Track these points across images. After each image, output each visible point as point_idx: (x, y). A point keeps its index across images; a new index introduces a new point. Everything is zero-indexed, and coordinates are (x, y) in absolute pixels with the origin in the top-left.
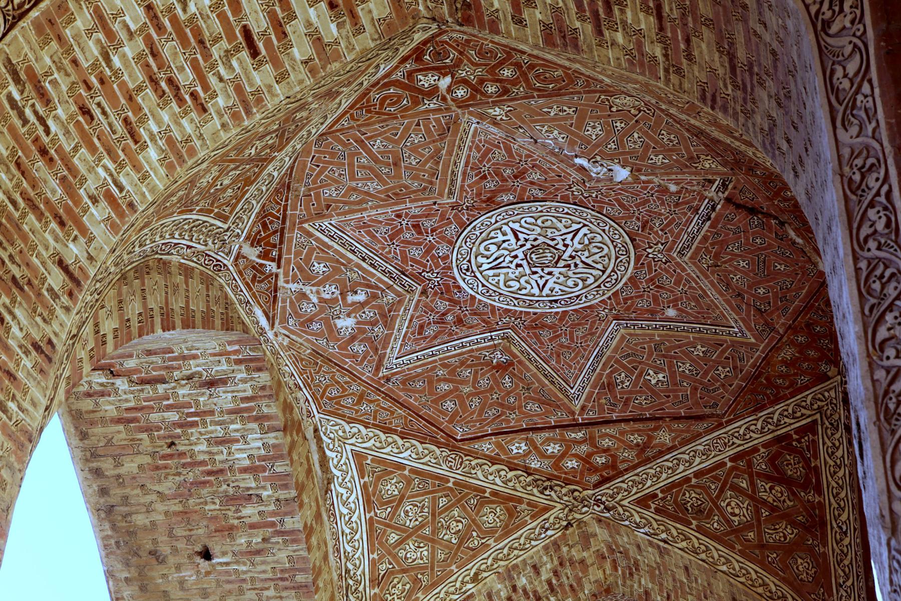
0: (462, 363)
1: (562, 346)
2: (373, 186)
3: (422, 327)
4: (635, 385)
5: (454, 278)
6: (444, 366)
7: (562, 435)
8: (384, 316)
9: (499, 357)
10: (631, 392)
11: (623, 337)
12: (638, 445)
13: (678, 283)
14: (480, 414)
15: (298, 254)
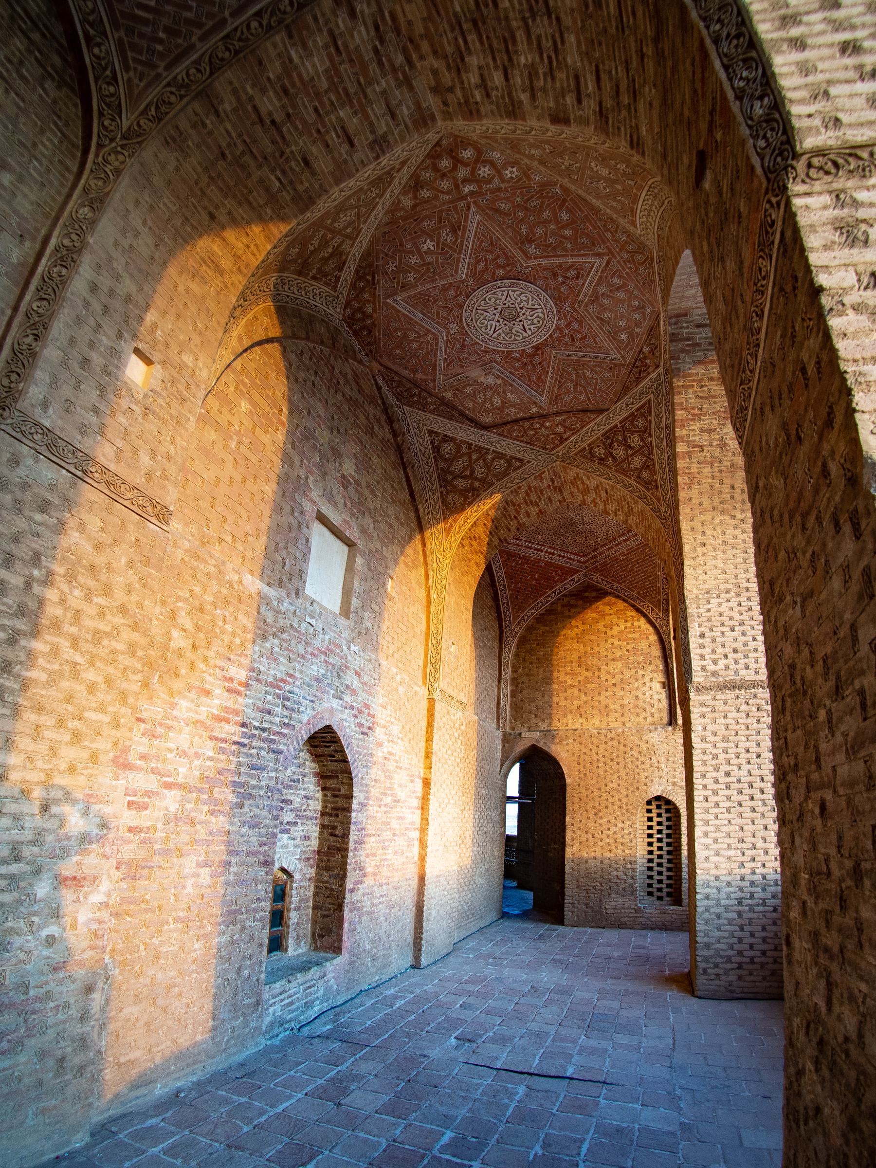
0: (554, 248)
1: (492, 253)
2: (588, 373)
3: (577, 278)
4: (439, 234)
5: (556, 305)
6: (565, 250)
7: (480, 187)
8: (597, 298)
9: (532, 249)
10: (440, 228)
11: (456, 272)
12: (422, 188)
13: (438, 313)
14: (543, 203)
15: (631, 349)
